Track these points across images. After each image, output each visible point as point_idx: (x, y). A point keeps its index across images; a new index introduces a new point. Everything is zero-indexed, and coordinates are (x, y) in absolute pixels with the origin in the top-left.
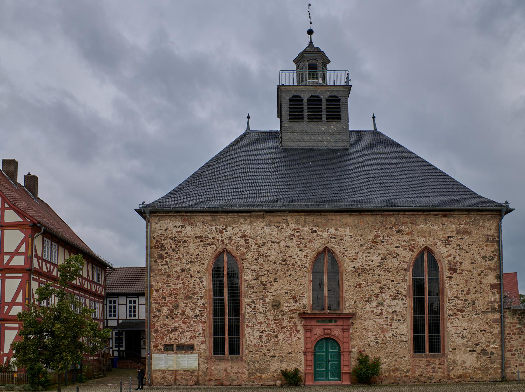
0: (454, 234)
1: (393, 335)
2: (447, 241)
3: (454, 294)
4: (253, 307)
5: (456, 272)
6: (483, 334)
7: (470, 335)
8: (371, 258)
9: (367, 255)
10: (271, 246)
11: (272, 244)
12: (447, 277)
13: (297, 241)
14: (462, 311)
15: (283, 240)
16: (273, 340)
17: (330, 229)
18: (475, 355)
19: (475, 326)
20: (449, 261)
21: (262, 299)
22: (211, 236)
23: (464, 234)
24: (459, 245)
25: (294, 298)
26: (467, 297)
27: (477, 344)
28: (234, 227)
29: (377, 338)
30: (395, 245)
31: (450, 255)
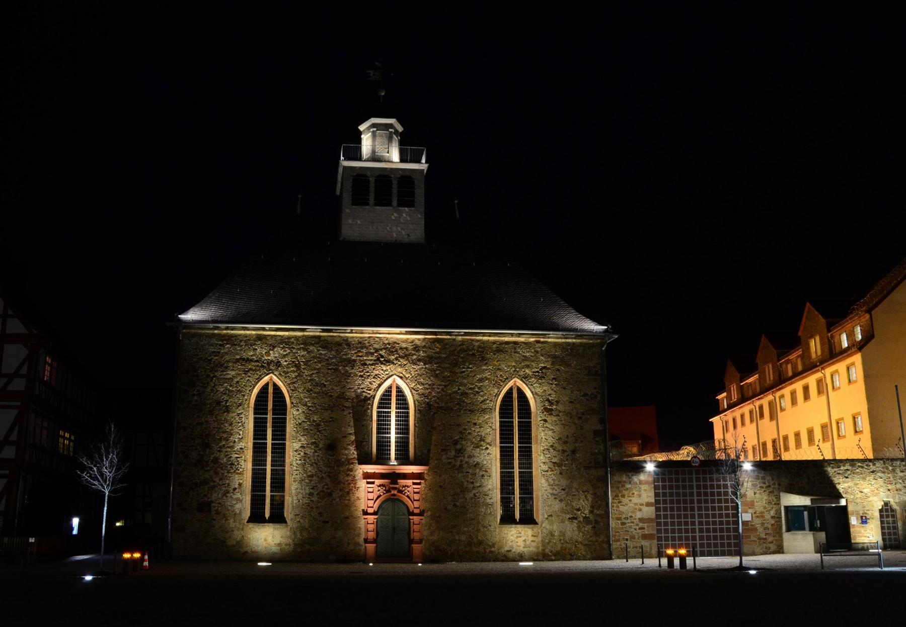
27: (578, 510)
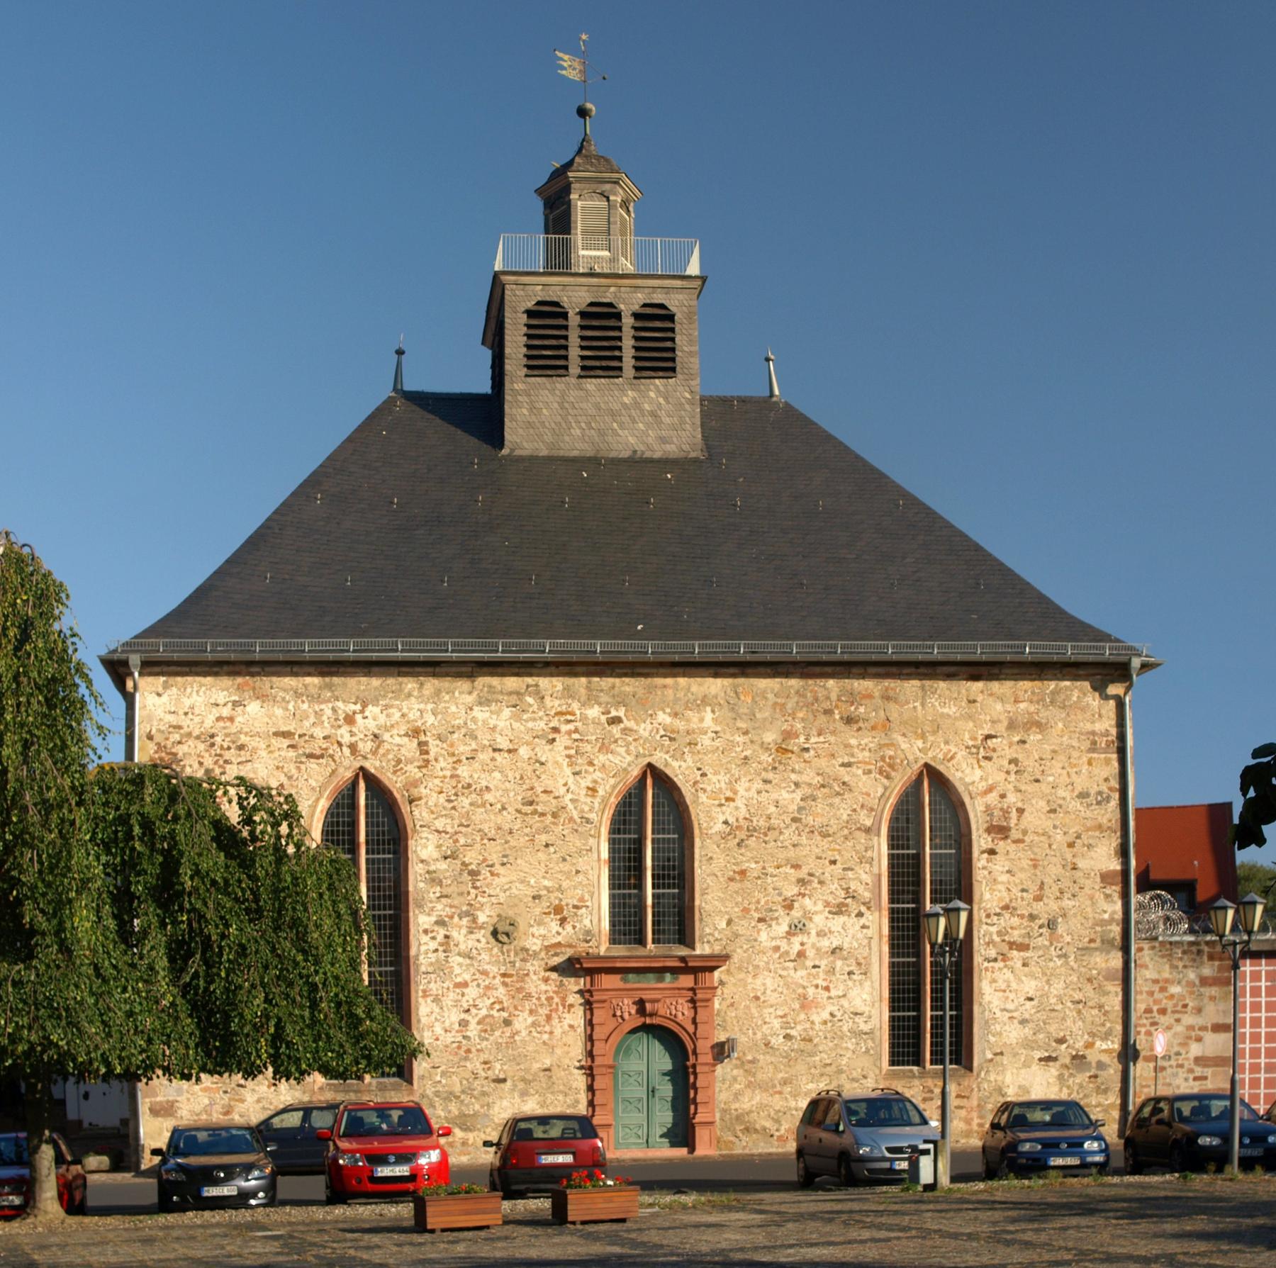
0: (1001, 728)
1: (832, 1015)
2: (983, 749)
3: (1001, 899)
4: (440, 938)
5: (1007, 837)
6: (1079, 1012)
7: (1042, 1016)
8: (774, 796)
9: (760, 785)
10: (493, 759)
11: (496, 755)
12: (983, 852)
13: (566, 748)
14: (1023, 947)
15: (528, 744)
16: (497, 1033)
17: (660, 713)
18: (1053, 1070)
19: (1058, 987)
20: (988, 807)
21: (467, 914)
22: (319, 732)
23: (1027, 730)
24: (1013, 761)
25: (558, 910)
26: (1038, 907)
27: (1061, 1041)
28: (387, 707)
29: (786, 1025)
30: (840, 760)
31: (990, 789)
